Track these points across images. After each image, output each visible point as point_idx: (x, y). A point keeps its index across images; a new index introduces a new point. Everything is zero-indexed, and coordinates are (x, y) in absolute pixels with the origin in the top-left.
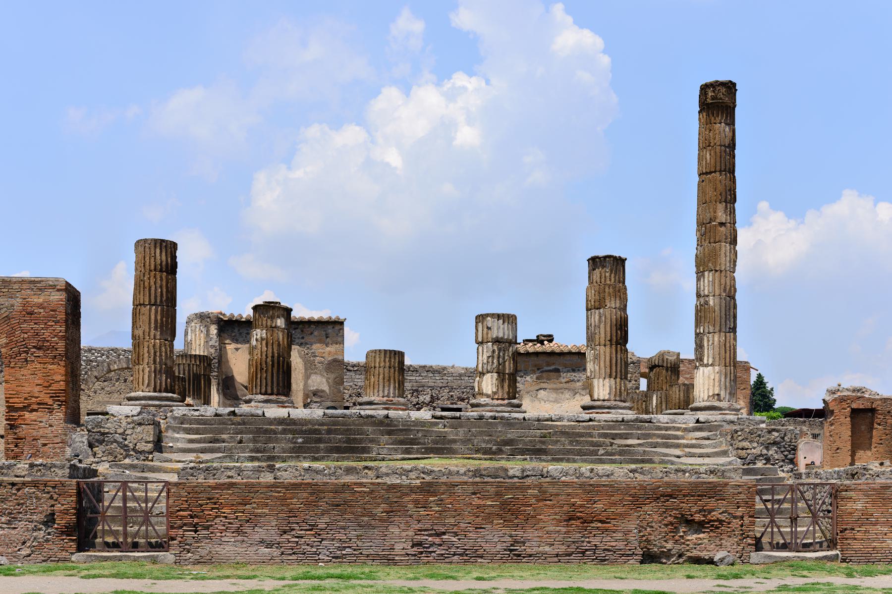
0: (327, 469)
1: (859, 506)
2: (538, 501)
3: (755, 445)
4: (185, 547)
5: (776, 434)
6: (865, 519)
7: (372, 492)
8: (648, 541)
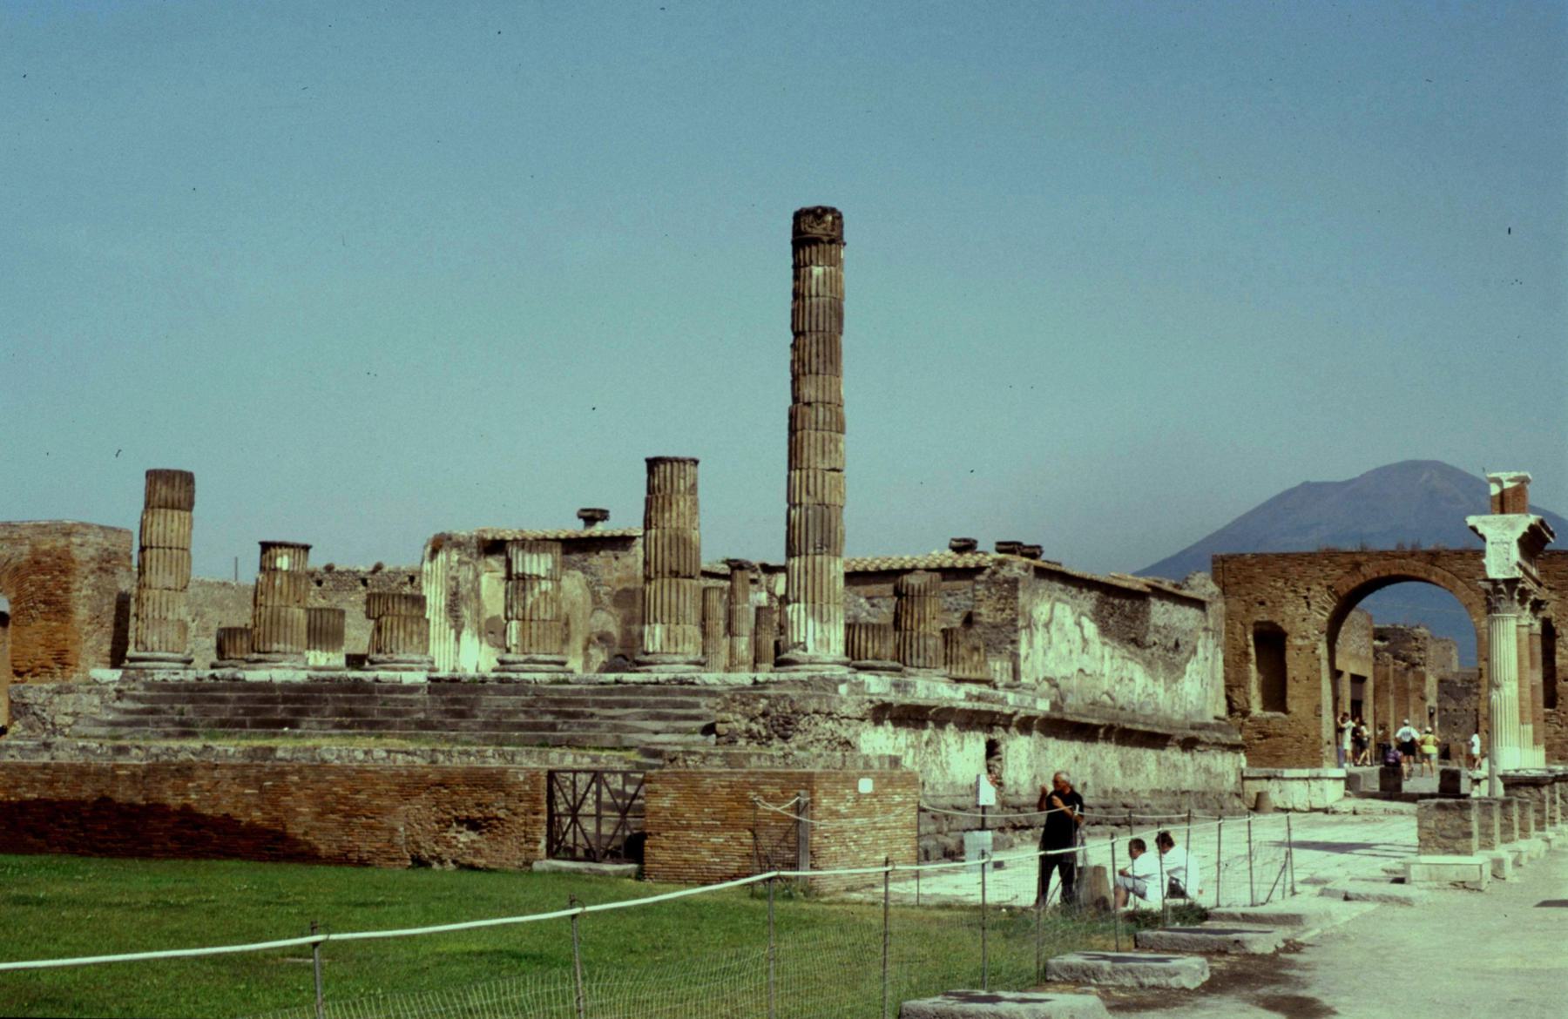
1: (667, 804)
2: (300, 789)
3: (739, 717)
5: (764, 702)
7: (134, 775)
8: (416, 843)
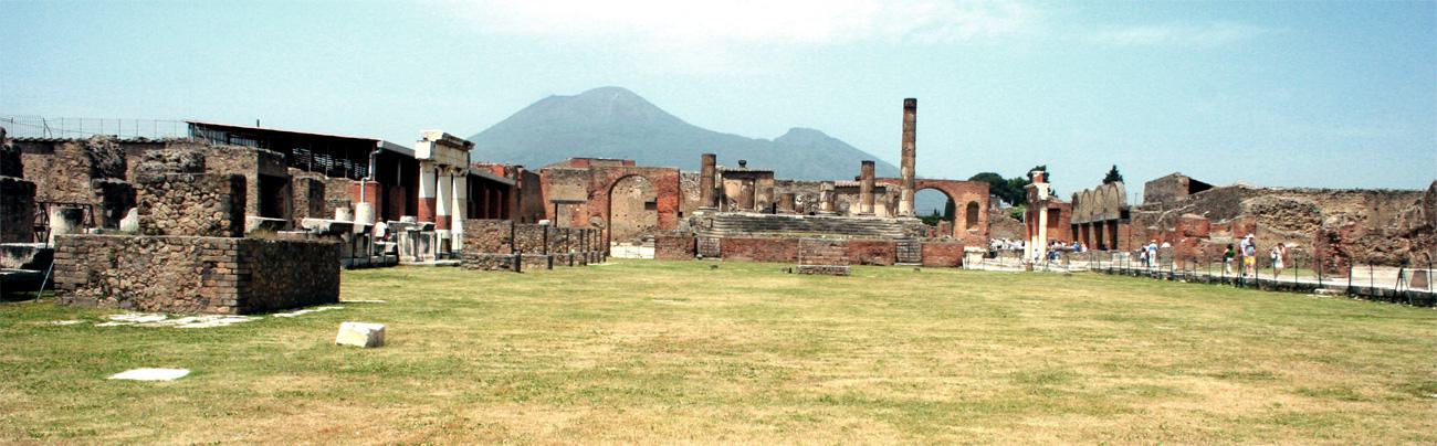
0: (768, 235)
4: (726, 256)
6: (931, 254)
